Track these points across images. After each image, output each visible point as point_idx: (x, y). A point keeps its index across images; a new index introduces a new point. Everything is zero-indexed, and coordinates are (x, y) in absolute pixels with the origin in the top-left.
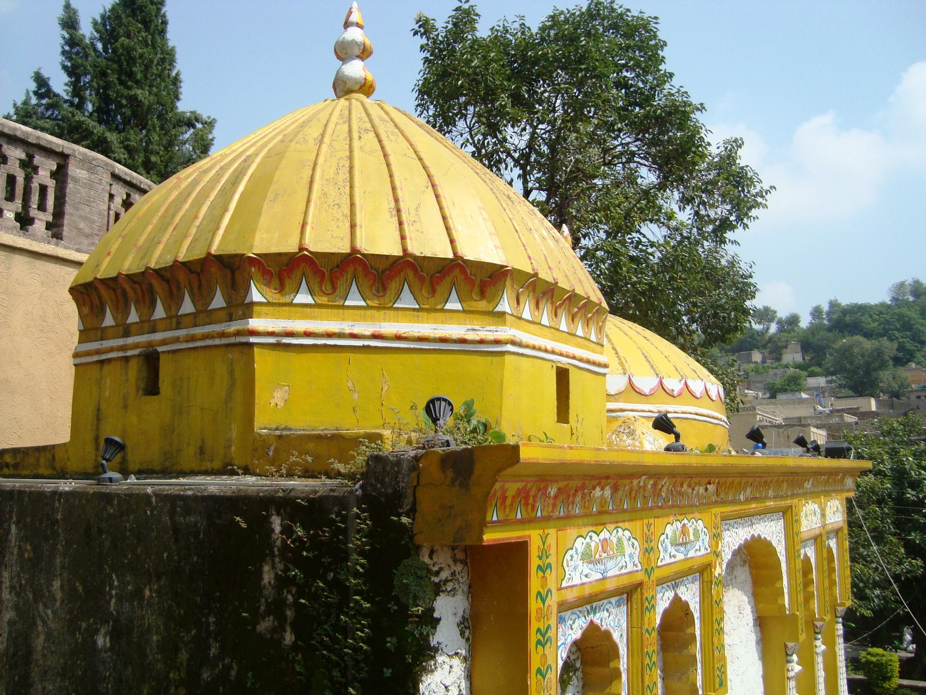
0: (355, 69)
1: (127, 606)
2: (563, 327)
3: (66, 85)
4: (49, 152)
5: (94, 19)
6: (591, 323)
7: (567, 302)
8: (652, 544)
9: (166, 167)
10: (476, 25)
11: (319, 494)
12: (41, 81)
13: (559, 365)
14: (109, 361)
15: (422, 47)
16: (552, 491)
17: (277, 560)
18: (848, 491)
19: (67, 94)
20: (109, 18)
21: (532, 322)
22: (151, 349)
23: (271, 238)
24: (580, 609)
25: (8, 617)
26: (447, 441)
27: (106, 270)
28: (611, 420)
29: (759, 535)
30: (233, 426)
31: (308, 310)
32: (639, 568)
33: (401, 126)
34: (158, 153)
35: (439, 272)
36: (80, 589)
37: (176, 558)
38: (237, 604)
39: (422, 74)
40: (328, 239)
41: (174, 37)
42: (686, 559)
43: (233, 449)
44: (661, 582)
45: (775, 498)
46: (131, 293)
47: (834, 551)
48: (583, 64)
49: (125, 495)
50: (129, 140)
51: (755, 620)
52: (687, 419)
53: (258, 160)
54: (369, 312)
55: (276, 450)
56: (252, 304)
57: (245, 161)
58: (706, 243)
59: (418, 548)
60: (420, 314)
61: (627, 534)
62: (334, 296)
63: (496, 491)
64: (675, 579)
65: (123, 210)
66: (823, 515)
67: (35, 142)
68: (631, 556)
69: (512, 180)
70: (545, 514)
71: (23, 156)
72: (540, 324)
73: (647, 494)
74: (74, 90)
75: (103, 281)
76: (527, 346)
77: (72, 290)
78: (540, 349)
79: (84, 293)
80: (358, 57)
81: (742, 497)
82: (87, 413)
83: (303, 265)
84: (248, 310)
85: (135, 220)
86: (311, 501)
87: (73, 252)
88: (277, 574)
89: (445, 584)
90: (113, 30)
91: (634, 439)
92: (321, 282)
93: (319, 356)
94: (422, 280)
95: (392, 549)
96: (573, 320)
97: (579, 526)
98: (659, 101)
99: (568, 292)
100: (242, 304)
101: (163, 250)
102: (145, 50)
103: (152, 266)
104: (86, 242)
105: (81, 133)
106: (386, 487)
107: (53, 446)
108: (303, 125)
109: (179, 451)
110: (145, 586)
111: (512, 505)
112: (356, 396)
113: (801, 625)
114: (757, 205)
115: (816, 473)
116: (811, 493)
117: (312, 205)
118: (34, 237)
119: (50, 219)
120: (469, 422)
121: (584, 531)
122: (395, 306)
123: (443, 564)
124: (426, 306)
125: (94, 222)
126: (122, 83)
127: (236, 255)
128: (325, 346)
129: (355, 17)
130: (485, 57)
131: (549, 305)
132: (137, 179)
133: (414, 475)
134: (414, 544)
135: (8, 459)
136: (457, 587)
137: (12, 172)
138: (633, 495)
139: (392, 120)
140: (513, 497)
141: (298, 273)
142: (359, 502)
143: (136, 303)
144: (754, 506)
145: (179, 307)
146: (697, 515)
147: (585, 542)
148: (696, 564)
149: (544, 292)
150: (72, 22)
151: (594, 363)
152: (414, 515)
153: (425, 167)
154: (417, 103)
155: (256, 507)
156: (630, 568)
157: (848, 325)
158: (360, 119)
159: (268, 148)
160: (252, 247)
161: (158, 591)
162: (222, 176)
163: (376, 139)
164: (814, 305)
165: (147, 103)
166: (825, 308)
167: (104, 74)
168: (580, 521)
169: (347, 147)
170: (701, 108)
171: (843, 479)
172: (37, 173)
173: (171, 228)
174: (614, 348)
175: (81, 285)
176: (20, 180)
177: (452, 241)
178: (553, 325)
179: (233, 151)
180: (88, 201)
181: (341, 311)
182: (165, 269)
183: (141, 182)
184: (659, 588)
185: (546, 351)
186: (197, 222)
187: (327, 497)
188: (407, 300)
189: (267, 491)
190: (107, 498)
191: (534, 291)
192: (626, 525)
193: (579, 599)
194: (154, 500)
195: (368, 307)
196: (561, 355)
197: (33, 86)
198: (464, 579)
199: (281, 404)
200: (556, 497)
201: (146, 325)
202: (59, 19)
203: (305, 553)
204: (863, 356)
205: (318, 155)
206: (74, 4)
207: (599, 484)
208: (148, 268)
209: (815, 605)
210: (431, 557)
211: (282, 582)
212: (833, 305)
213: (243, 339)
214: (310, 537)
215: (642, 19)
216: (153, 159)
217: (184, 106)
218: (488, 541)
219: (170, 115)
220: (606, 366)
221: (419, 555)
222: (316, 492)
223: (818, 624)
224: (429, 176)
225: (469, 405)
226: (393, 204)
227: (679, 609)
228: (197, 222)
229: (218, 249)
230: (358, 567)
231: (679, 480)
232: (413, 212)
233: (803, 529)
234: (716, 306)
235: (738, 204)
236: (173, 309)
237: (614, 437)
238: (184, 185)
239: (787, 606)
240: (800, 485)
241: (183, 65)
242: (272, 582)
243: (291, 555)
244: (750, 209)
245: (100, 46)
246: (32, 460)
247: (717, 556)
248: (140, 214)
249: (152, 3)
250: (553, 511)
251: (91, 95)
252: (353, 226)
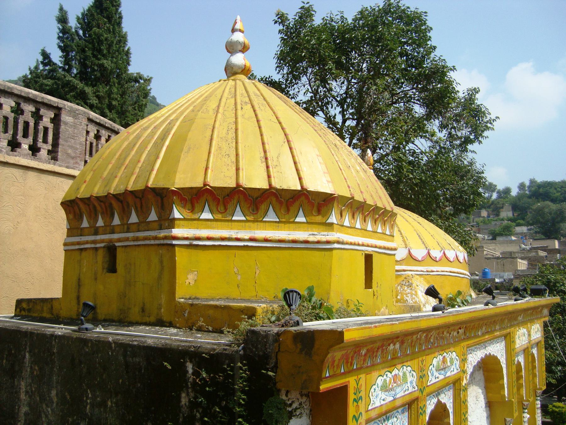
0: (239, 59)
1: (97, 410)
2: (369, 228)
3: (61, 57)
4: (49, 106)
5: (78, 16)
6: (386, 223)
7: (372, 212)
8: (424, 373)
9: (122, 108)
10: (314, 18)
11: (216, 351)
12: (45, 55)
13: (367, 253)
14: (86, 249)
15: (280, 31)
16: (363, 352)
17: (190, 390)
18: (545, 317)
19: (61, 63)
20: (87, 15)
21: (350, 227)
22: (111, 244)
23: (185, 178)
24: (379, 419)
25: (24, 410)
26: (298, 321)
27: (83, 193)
28: (398, 276)
29: (490, 354)
30: (162, 296)
31: (210, 223)
32: (416, 388)
33: (268, 99)
34: (116, 99)
35: (292, 198)
36: (68, 397)
37: (127, 383)
38: (165, 416)
39: (279, 47)
40: (221, 178)
41: (127, 26)
42: (445, 378)
43: (163, 310)
44: (428, 395)
45: (500, 329)
46: (99, 208)
47: (536, 355)
48: (380, 43)
49: (95, 341)
50: (99, 92)
51: (486, 404)
52: (445, 275)
53: (178, 124)
54: (247, 224)
56: (174, 219)
57: (170, 123)
58: (454, 151)
59: (279, 391)
60: (280, 224)
61: (409, 368)
62: (225, 213)
63: (328, 359)
64: (438, 391)
65: (95, 140)
66: (529, 335)
67: (40, 101)
68: (411, 382)
69: (335, 115)
70: (359, 366)
71: (33, 110)
72: (355, 228)
73: (422, 342)
74: (65, 61)
75: (82, 200)
76: (347, 243)
77: (62, 204)
78: (355, 244)
79: (71, 206)
80: (240, 51)
81: (480, 333)
82: (73, 281)
83: (206, 195)
84: (171, 223)
85: (101, 160)
86: (212, 356)
87: (64, 168)
88: (190, 399)
89: (295, 411)
90: (89, 23)
91: (411, 289)
92: (218, 204)
93: (217, 252)
94: (281, 203)
95: (263, 391)
96: (375, 223)
97: (379, 370)
98: (427, 64)
99: (373, 206)
100: (168, 219)
101: (118, 182)
102: (109, 35)
103: (112, 192)
104: (72, 161)
105: (70, 87)
106: (259, 351)
107: (52, 299)
108: (206, 99)
109: (129, 309)
110: (108, 399)
111: (338, 365)
112: (239, 277)
113: (515, 406)
114: (488, 128)
115: (525, 311)
116: (522, 322)
117: (212, 155)
118: (40, 160)
119: (50, 148)
120: (310, 301)
121: (382, 372)
122: (264, 220)
123: (294, 399)
124: (283, 220)
125: (77, 149)
126: (95, 56)
127: (164, 189)
128: (220, 246)
129: (238, 26)
130: (318, 39)
131: (361, 215)
132: (103, 121)
133: (276, 345)
134: (276, 388)
135: (24, 305)
136: (303, 411)
137: (26, 120)
138: (413, 344)
139: (262, 95)
140: (339, 360)
141: (203, 199)
142: (242, 358)
143: (102, 214)
144: (487, 337)
145: (128, 218)
146: (452, 349)
147: (383, 379)
148: (451, 380)
149: (357, 207)
150: (64, 19)
151: (388, 249)
152: (277, 370)
153: (283, 129)
154: (276, 65)
155: (177, 355)
156: (411, 390)
157: (541, 194)
158: (242, 94)
159: (184, 115)
161: (116, 403)
162: (155, 134)
163: (252, 109)
164: (520, 182)
165: (110, 68)
166: (527, 183)
167: (83, 51)
168: (380, 366)
169: (234, 115)
170: (454, 69)
171: (541, 311)
172: (42, 120)
173: (123, 168)
174: (399, 231)
175: (68, 201)
176: (32, 124)
177: (300, 179)
178: (363, 228)
179: (162, 116)
180: (73, 136)
181: (230, 223)
182: (120, 194)
183: (106, 123)
184: (428, 398)
185: (359, 245)
186: (140, 165)
187: (221, 354)
188: (271, 216)
189: (184, 346)
190: (85, 342)
191: (351, 208)
192: (409, 363)
193: (379, 414)
194: (113, 345)
195: (247, 221)
196: (368, 246)
197: (41, 58)
198: (307, 406)
199: (192, 283)
200: (365, 355)
201: (108, 228)
202: (56, 17)
203: (207, 389)
204: (550, 214)
205: (215, 121)
206: (65, 8)
207: (392, 342)
208: (109, 194)
209: (524, 391)
210: (287, 396)
211: (193, 405)
212: (532, 182)
213: (169, 242)
214: (211, 379)
215: (417, 13)
216: (114, 103)
217: (133, 69)
218: (323, 389)
219: (124, 75)
220: (395, 249)
221: (279, 395)
222: (214, 350)
223: (525, 403)
224: (285, 135)
225: (311, 291)
226: (262, 154)
227: (441, 409)
228: (140, 165)
229: (152, 184)
230: (241, 401)
231: (441, 330)
232: (275, 159)
233: (517, 346)
234: (461, 191)
235: (476, 129)
236: (125, 219)
237: (399, 288)
238: (132, 137)
239: (506, 395)
240: (516, 319)
241: (132, 44)
242: (187, 404)
243: (199, 389)
244: (483, 131)
245: (81, 32)
246: (38, 307)
247: (464, 373)
248: (104, 156)
249: (113, 6)
250: (363, 363)
251: (75, 63)
252: (237, 169)
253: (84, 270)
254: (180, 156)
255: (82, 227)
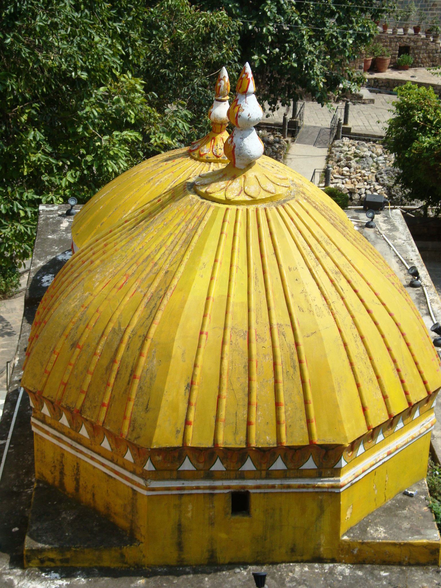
30: (322, 537)
43: (322, 549)
55: (360, 550)
160: (346, 438)
229: (318, 439)
253: (190, 515)
254: (336, 398)
255: (180, 469)
